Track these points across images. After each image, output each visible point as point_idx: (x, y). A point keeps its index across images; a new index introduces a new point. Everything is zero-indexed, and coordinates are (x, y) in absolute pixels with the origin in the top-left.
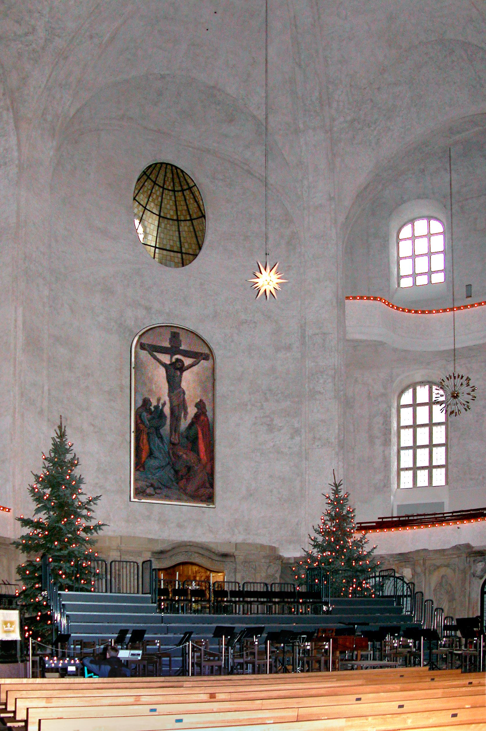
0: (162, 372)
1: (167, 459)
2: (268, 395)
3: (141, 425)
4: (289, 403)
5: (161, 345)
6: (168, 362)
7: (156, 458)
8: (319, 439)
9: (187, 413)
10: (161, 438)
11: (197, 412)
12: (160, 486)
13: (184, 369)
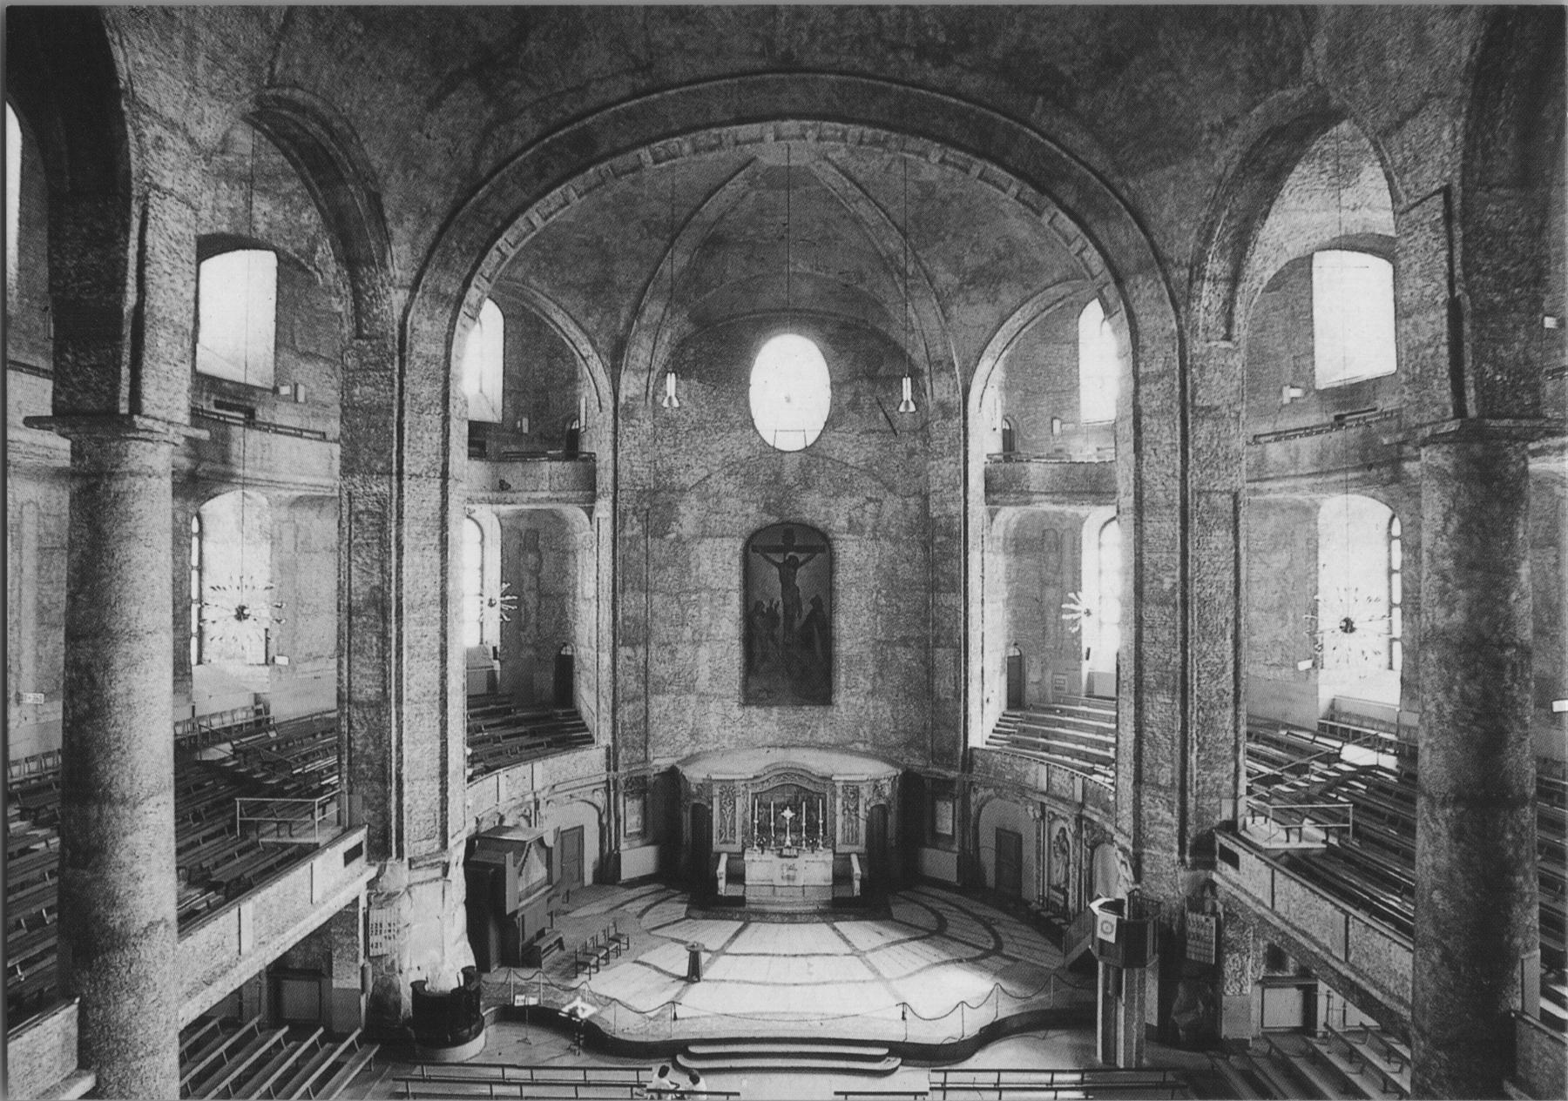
0: (775, 571)
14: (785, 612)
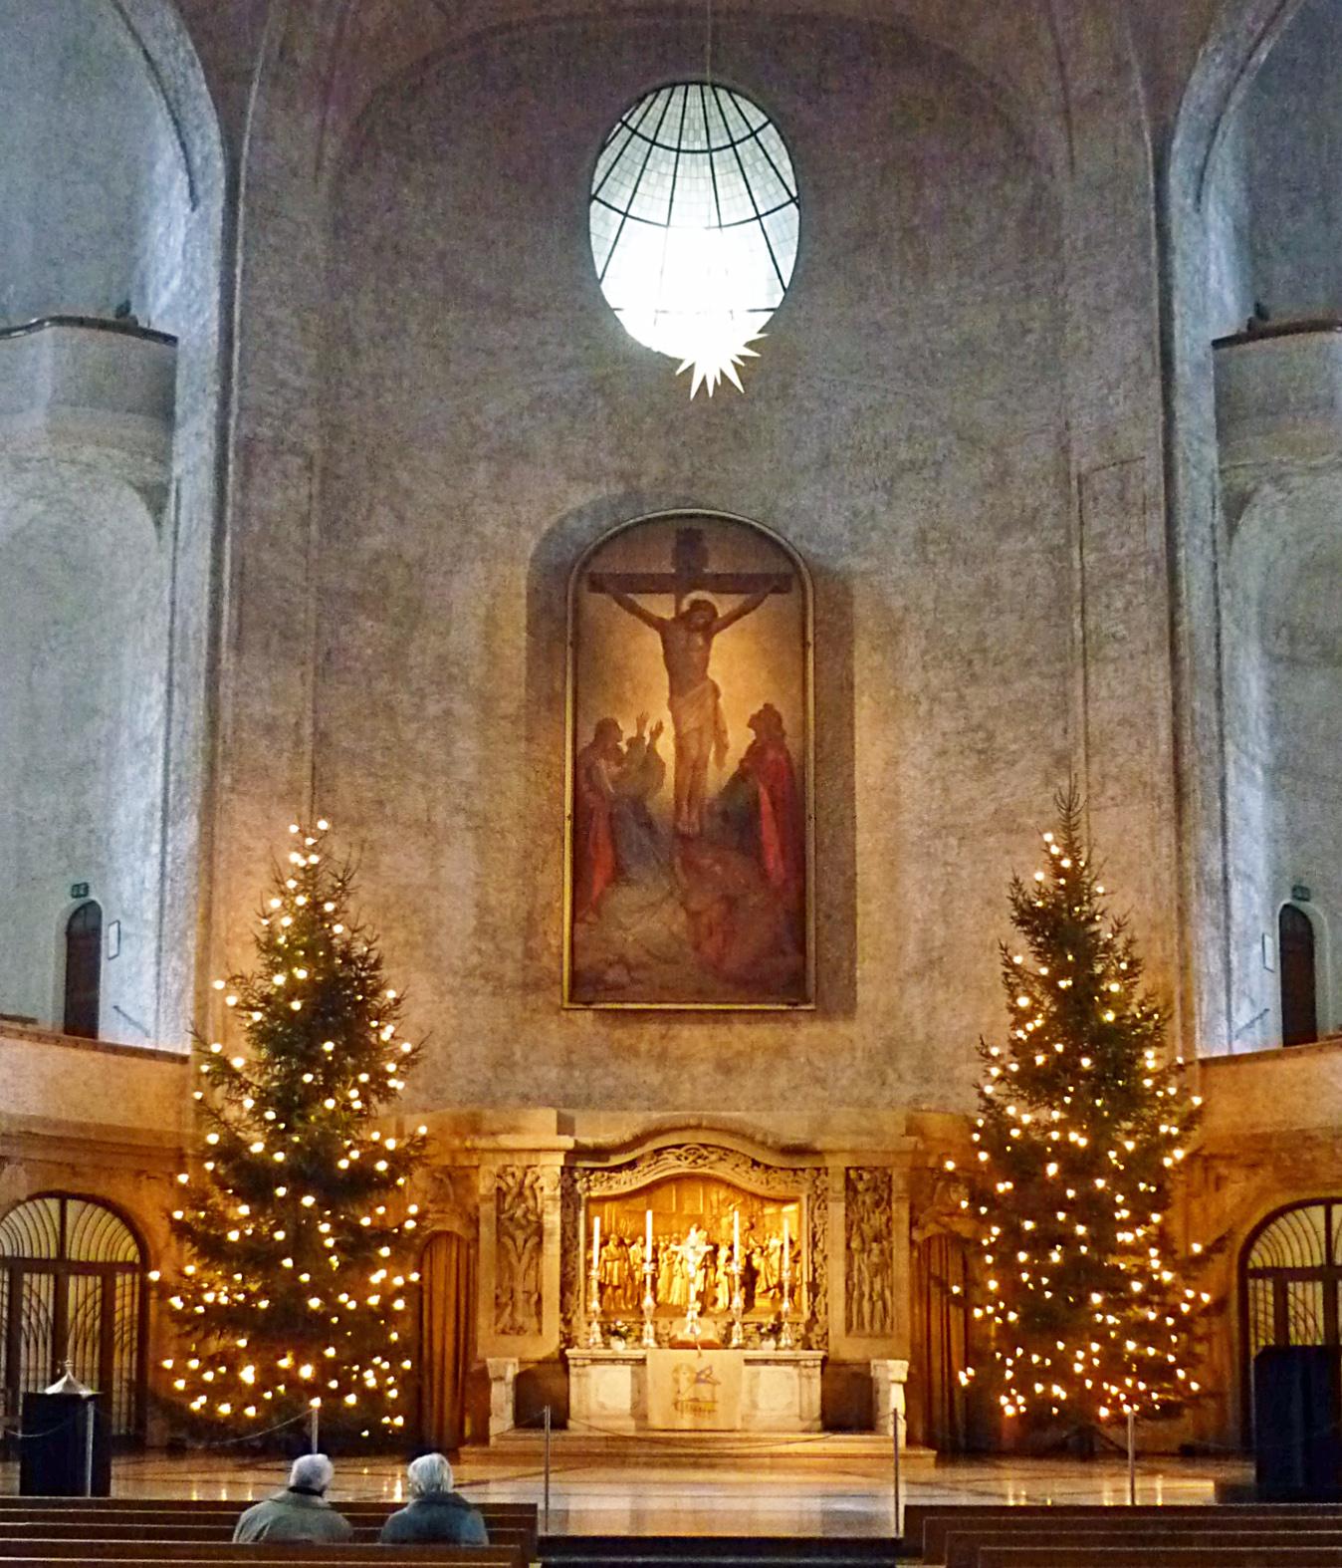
0: (653, 641)
1: (665, 882)
2: (977, 668)
3: (590, 796)
4: (1036, 680)
5: (643, 570)
6: (668, 614)
7: (629, 882)
8: (1117, 779)
9: (726, 747)
10: (649, 825)
11: (755, 742)
12: (646, 958)
13: (715, 624)
14: (681, 751)
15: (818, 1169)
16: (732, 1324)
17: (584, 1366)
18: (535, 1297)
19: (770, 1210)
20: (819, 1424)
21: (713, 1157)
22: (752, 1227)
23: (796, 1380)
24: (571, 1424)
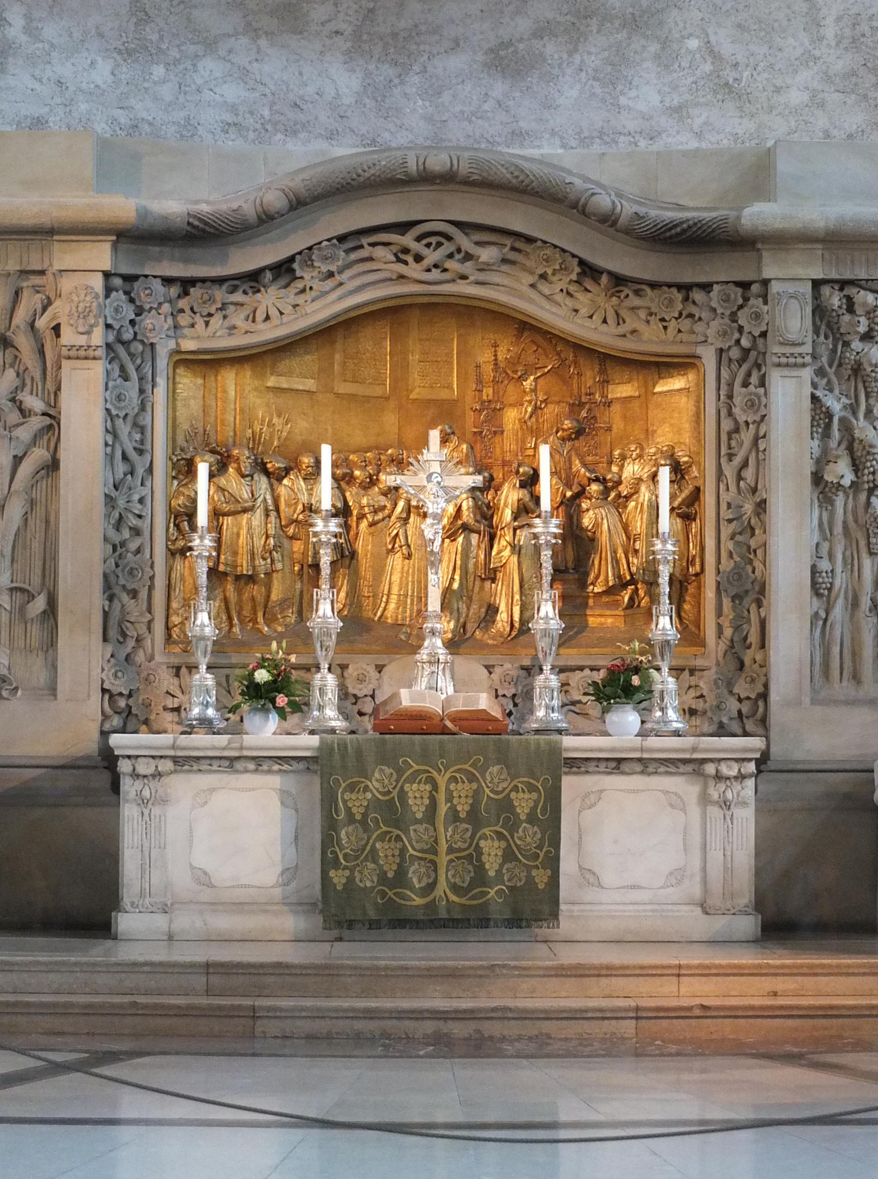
15: (745, 286)
16: (531, 670)
17: (158, 775)
18: (40, 604)
19: (622, 390)
20: (748, 925)
21: (487, 255)
22: (579, 433)
23: (695, 811)
24: (124, 922)
